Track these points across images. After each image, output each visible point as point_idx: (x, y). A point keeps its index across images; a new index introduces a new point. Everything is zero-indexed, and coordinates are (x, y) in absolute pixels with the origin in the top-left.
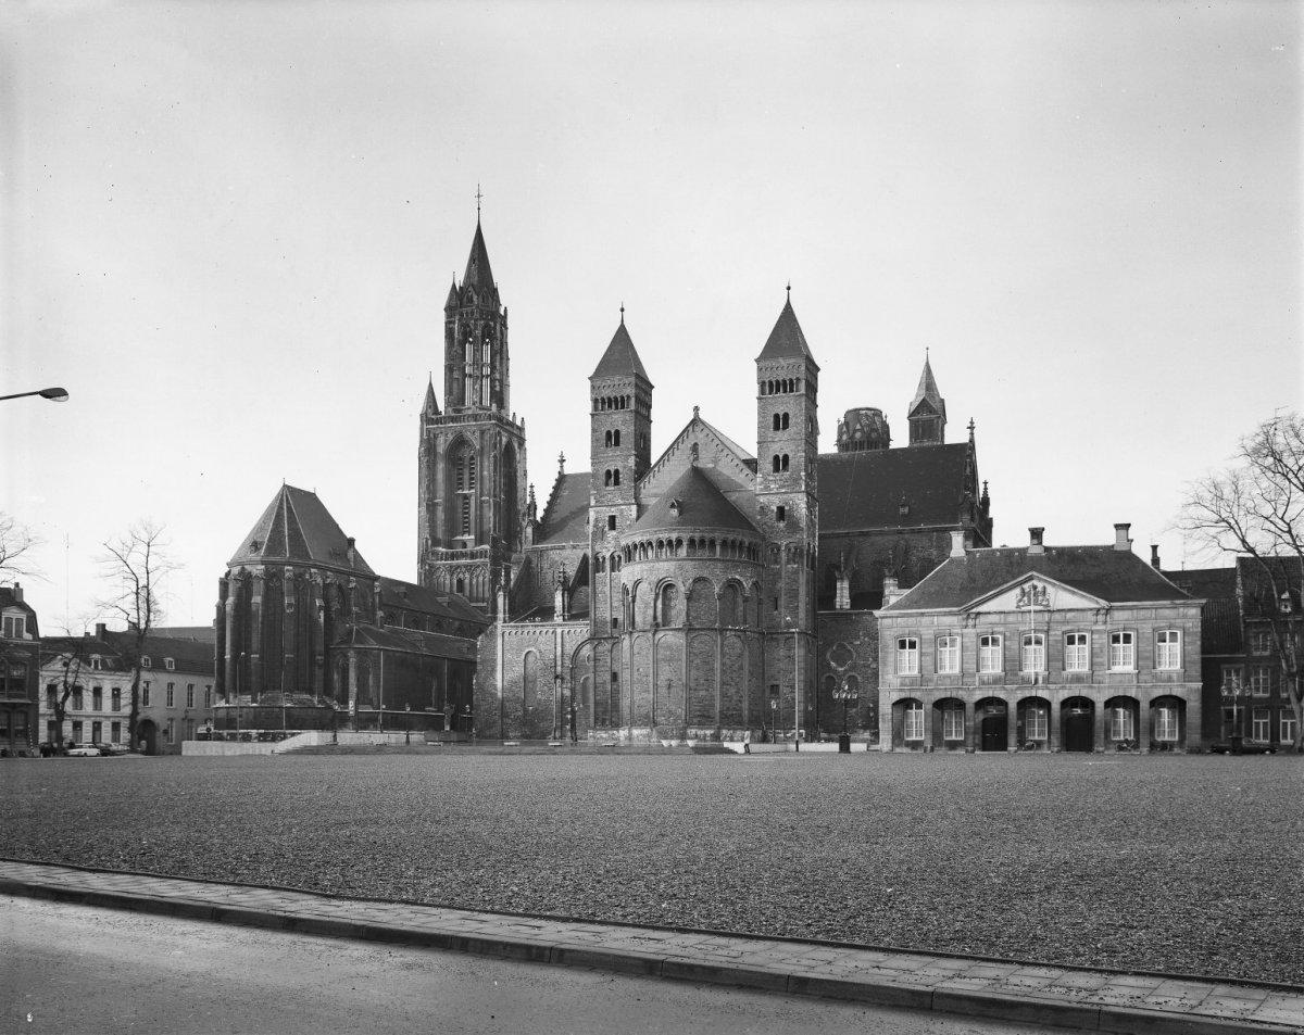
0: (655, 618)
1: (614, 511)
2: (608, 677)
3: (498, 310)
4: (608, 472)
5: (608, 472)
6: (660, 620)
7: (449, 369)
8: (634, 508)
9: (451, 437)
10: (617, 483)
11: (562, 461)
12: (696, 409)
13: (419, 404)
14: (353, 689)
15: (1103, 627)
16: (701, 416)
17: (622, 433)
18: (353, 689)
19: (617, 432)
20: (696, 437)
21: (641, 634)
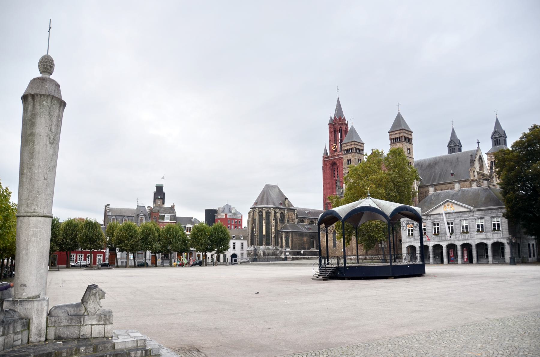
3: (345, 122)
7: (330, 141)
13: (322, 155)
14: (284, 244)
15: (473, 218)
17: (352, 160)
18: (284, 244)
19: (350, 160)
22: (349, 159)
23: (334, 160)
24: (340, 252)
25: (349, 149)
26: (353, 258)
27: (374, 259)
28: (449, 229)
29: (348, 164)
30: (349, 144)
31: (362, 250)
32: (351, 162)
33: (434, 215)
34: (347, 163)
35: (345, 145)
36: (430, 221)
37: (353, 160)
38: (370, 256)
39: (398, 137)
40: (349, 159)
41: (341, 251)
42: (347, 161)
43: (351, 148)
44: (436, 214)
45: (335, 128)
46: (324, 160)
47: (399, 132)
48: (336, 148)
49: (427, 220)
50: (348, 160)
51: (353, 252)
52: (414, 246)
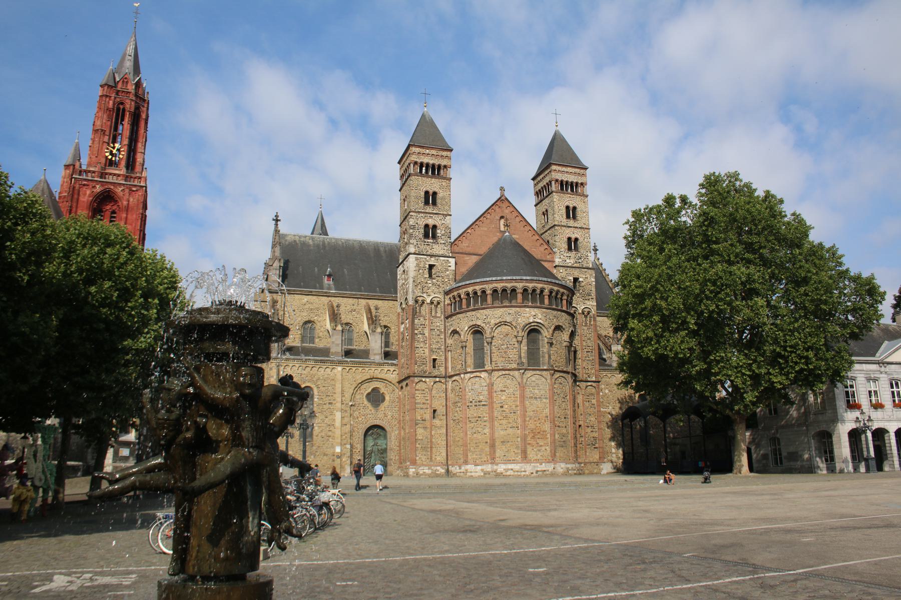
0: (520, 357)
1: (432, 261)
2: (428, 415)
4: (427, 226)
5: (427, 226)
6: (524, 360)
8: (452, 261)
9: (99, 188)
10: (434, 236)
11: (277, 220)
12: (502, 189)
16: (507, 194)
17: (439, 196)
19: (435, 194)
20: (503, 211)
21: (501, 373)
22: (431, 192)
23: (112, 187)
24: (325, 455)
25: (433, 165)
26: (507, 470)
27: (570, 472)
28: (894, 397)
29: (427, 202)
30: (434, 152)
31: (541, 446)
32: (438, 201)
33: (892, 363)
34: (423, 200)
35: (421, 150)
36: (886, 376)
37: (443, 198)
38: (563, 465)
39: (575, 181)
40: (431, 192)
41: (330, 451)
42: (423, 194)
43: (439, 166)
44: (896, 364)
45: (122, 104)
46: (74, 176)
47: (577, 170)
48: (121, 156)
49: (881, 373)
50: (427, 193)
51: (499, 453)
52: (851, 431)
